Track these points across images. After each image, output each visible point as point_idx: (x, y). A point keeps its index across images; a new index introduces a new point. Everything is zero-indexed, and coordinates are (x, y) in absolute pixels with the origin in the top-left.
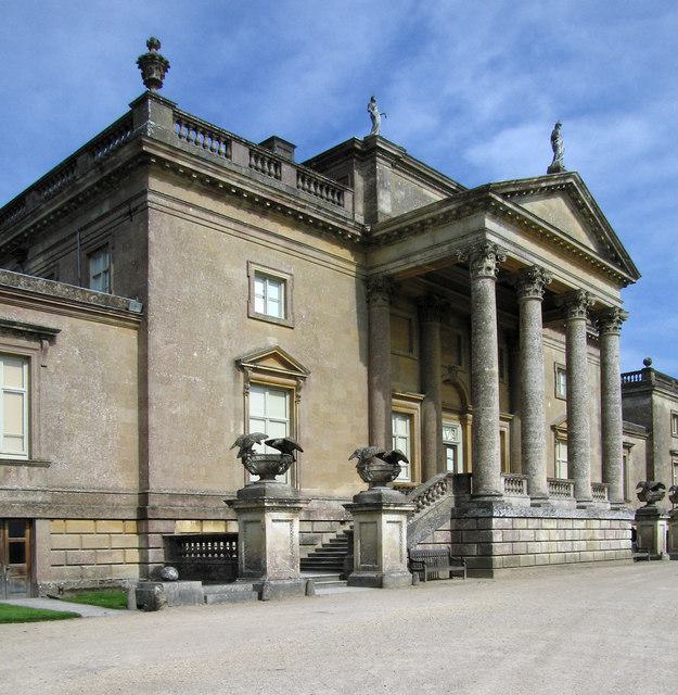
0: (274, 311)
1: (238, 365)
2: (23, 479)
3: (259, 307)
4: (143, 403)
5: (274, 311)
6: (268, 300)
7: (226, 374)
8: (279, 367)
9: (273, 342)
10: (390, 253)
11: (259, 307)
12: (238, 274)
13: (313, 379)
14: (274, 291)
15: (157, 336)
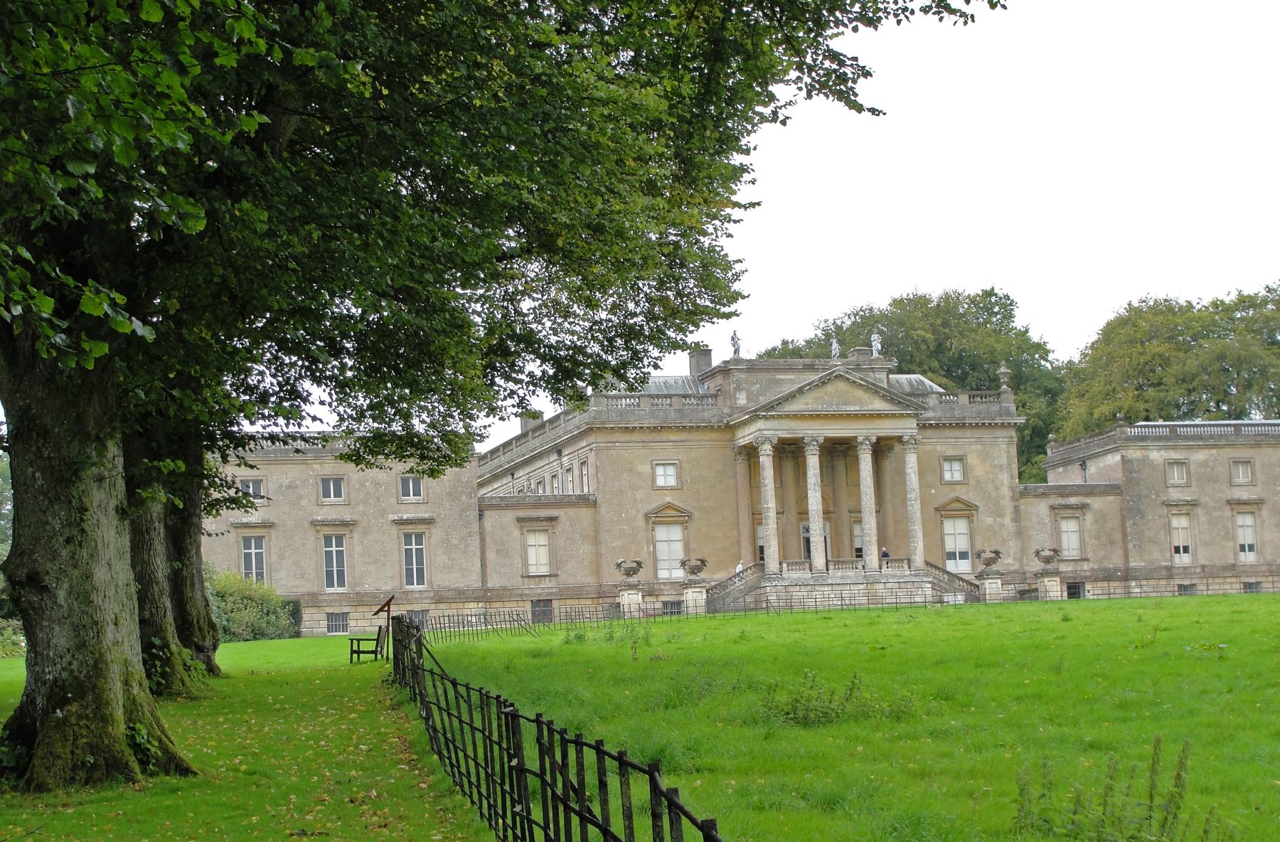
0: (672, 482)
1: (647, 517)
2: (547, 584)
3: (660, 482)
4: (596, 541)
5: (672, 482)
6: (666, 477)
7: (641, 522)
8: (673, 512)
9: (668, 499)
10: (740, 433)
11: (660, 482)
12: (645, 469)
13: (696, 515)
14: (671, 471)
15: (603, 511)
